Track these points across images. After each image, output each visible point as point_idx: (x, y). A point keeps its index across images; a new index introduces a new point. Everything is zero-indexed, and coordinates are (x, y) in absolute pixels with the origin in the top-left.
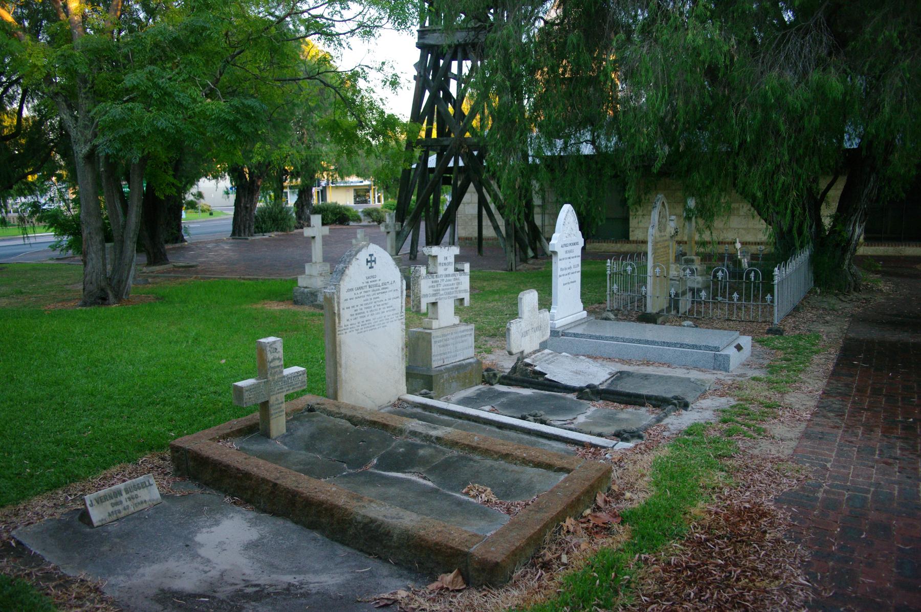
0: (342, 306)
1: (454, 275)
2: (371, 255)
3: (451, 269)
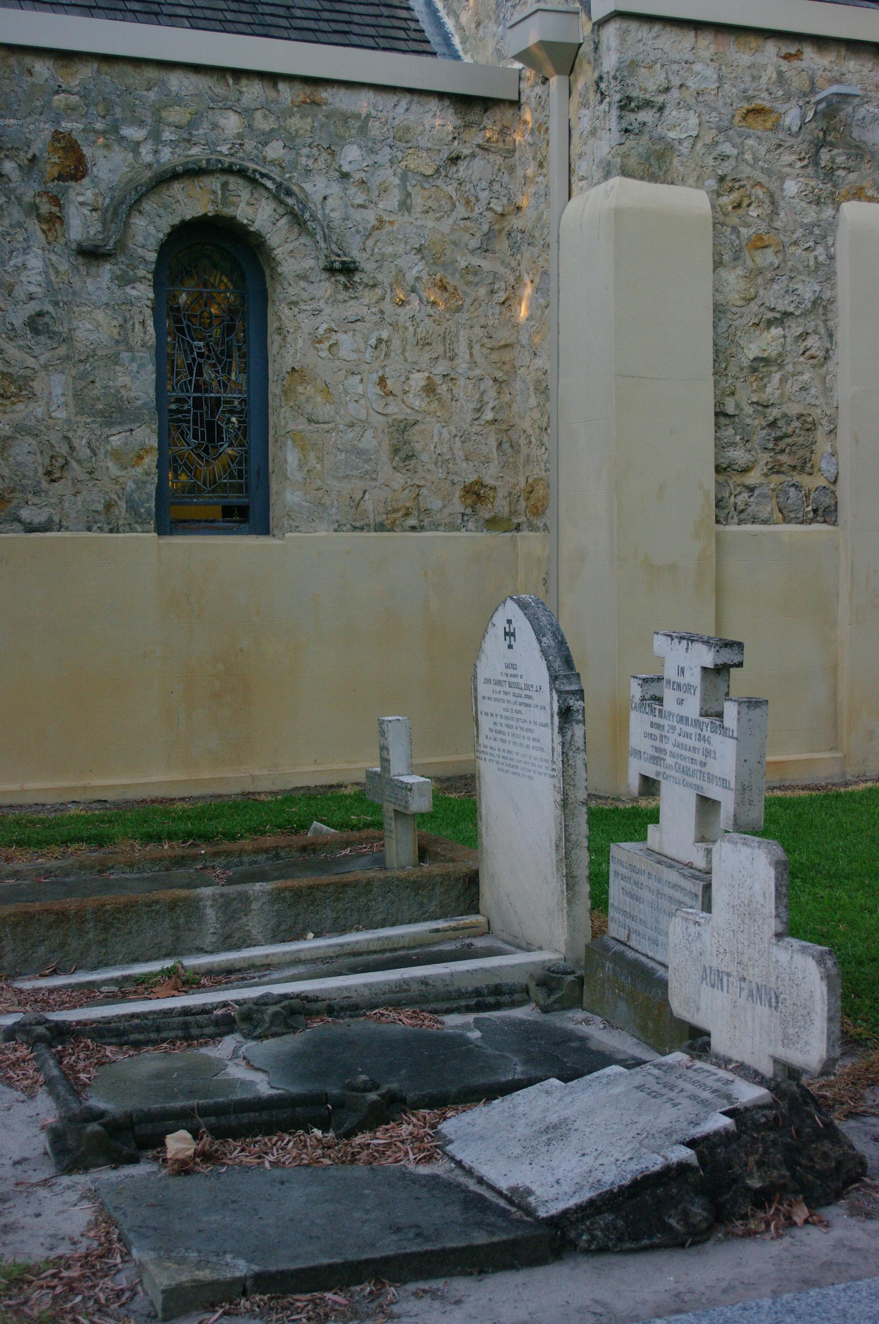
1: (696, 723)
3: (692, 706)
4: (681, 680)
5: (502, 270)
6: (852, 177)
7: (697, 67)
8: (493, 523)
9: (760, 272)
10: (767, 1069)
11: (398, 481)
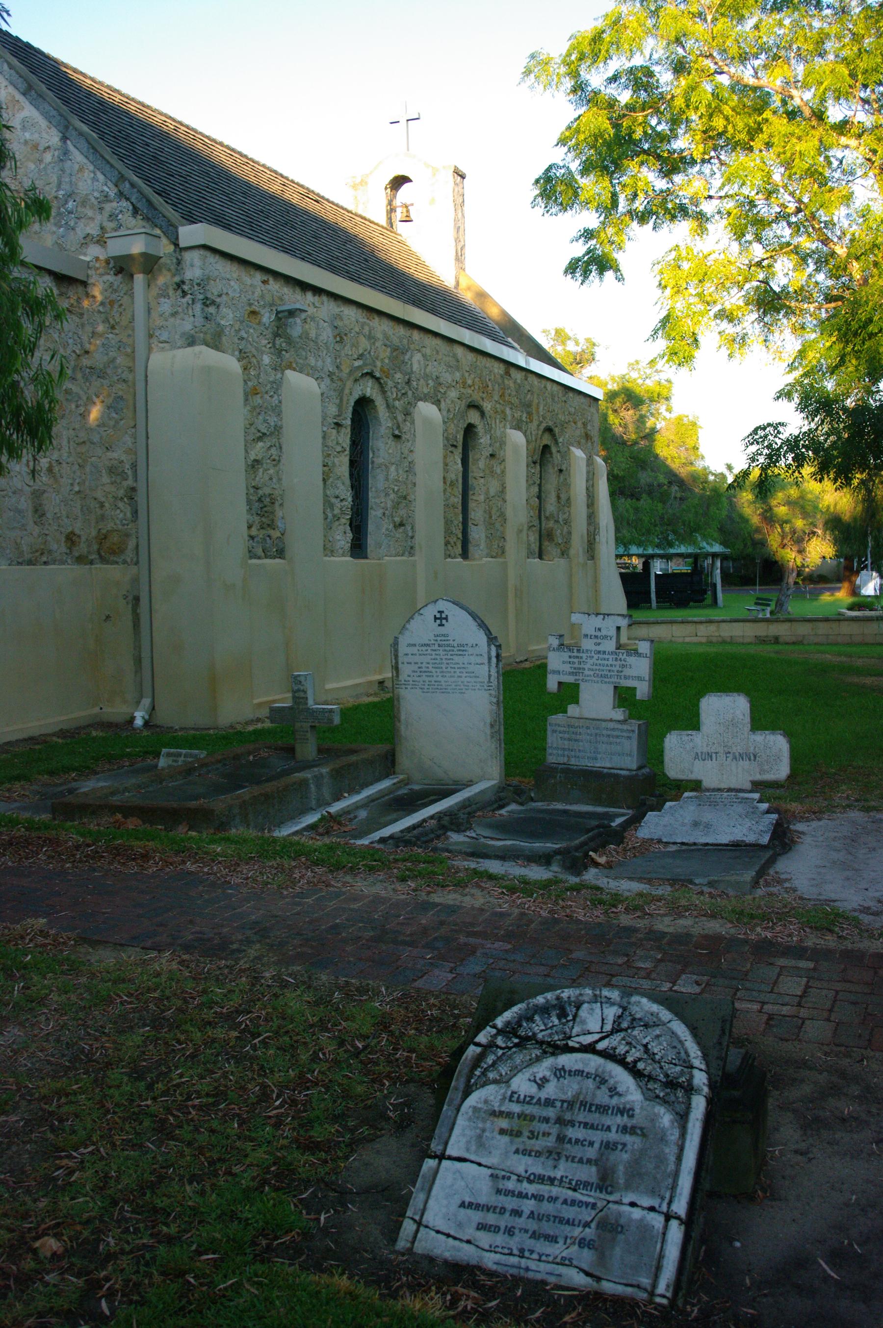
0: (400, 660)
2: (441, 612)
3: (611, 646)
4: (599, 634)
5: (81, 393)
6: (287, 355)
7: (232, 283)
8: (81, 560)
9: (254, 408)
10: (748, 786)
11: (37, 530)
